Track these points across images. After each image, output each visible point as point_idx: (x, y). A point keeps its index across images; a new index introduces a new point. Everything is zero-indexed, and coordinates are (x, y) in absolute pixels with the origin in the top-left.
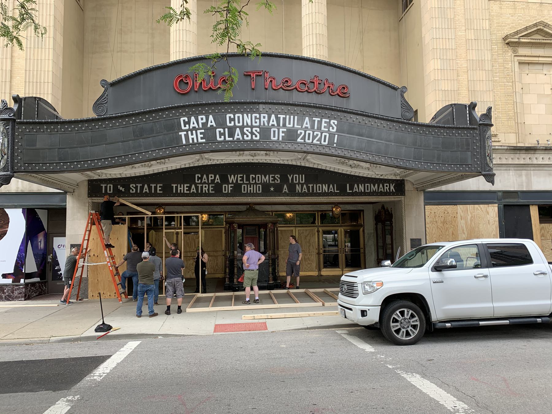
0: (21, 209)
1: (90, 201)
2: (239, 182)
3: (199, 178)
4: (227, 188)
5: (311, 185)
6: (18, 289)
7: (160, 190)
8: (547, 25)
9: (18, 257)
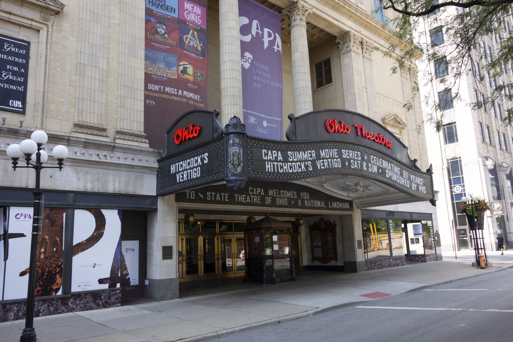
0: (117, 211)
1: (177, 205)
2: (275, 196)
3: (251, 191)
4: (268, 200)
5: (312, 201)
6: (115, 294)
7: (227, 199)
8: (397, 116)
9: (114, 260)
